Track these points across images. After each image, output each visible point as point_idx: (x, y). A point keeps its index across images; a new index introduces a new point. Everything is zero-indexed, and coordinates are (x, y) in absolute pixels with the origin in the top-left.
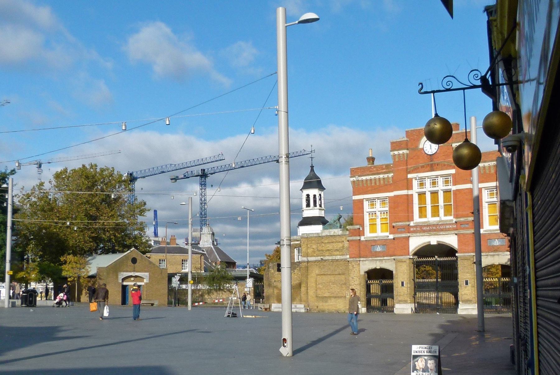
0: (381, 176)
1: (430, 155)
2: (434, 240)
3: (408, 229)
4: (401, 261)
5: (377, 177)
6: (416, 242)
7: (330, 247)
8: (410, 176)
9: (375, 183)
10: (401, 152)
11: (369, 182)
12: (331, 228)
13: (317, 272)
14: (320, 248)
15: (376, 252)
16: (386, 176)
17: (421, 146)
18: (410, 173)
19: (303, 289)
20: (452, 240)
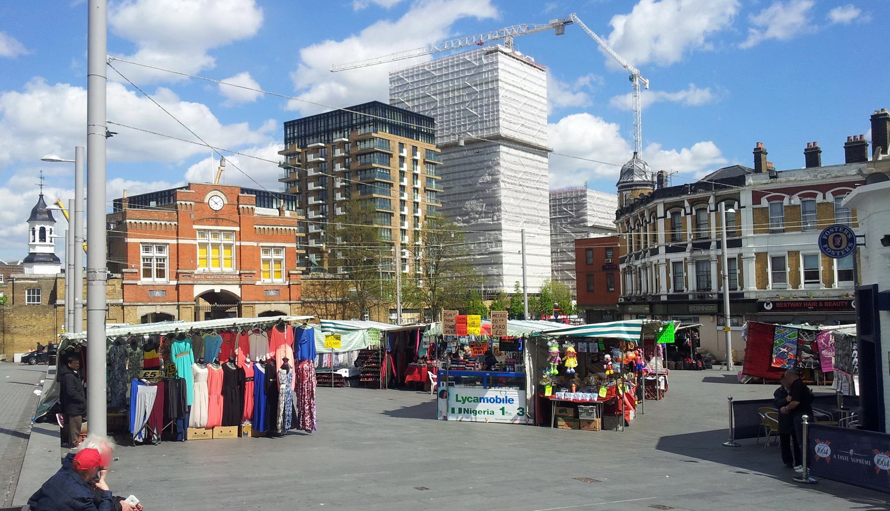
2: (217, 289)
3: (189, 275)
6: (198, 290)
8: (195, 227)
15: (154, 297)
17: (206, 201)
20: (235, 290)
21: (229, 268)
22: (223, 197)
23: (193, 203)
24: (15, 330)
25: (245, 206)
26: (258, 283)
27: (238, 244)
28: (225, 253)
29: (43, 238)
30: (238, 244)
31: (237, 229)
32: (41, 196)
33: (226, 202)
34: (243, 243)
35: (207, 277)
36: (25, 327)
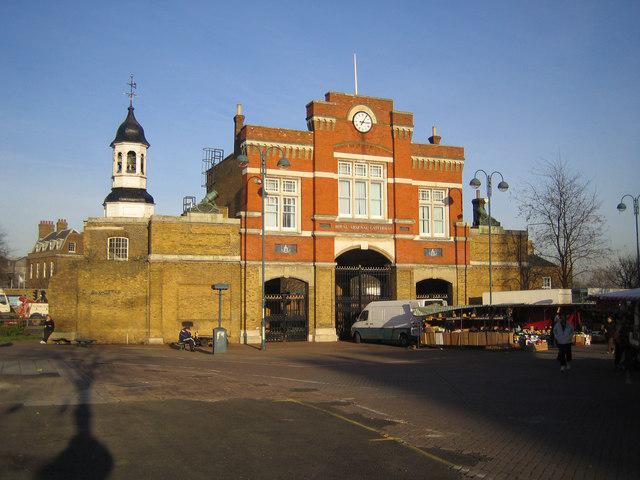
0: (294, 147)
1: (363, 133)
3: (329, 225)
4: (324, 269)
5: (288, 146)
6: (341, 245)
7: (204, 240)
8: (337, 155)
9: (284, 155)
10: (328, 120)
11: (274, 151)
12: (205, 212)
13: (180, 279)
14: (185, 241)
16: (301, 147)
17: (350, 118)
18: (336, 150)
19: (154, 307)
20: (386, 247)
21: (378, 212)
22: (372, 114)
23: (334, 120)
24: (94, 298)
25: (401, 128)
26: (417, 238)
27: (391, 181)
28: (374, 191)
29: (132, 169)
30: (391, 181)
31: (390, 160)
32: (131, 110)
33: (375, 122)
34: (398, 180)
35: (351, 227)
36: (108, 293)
